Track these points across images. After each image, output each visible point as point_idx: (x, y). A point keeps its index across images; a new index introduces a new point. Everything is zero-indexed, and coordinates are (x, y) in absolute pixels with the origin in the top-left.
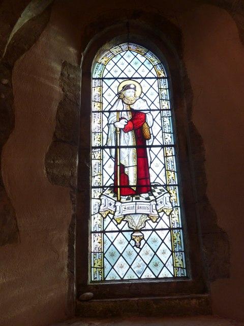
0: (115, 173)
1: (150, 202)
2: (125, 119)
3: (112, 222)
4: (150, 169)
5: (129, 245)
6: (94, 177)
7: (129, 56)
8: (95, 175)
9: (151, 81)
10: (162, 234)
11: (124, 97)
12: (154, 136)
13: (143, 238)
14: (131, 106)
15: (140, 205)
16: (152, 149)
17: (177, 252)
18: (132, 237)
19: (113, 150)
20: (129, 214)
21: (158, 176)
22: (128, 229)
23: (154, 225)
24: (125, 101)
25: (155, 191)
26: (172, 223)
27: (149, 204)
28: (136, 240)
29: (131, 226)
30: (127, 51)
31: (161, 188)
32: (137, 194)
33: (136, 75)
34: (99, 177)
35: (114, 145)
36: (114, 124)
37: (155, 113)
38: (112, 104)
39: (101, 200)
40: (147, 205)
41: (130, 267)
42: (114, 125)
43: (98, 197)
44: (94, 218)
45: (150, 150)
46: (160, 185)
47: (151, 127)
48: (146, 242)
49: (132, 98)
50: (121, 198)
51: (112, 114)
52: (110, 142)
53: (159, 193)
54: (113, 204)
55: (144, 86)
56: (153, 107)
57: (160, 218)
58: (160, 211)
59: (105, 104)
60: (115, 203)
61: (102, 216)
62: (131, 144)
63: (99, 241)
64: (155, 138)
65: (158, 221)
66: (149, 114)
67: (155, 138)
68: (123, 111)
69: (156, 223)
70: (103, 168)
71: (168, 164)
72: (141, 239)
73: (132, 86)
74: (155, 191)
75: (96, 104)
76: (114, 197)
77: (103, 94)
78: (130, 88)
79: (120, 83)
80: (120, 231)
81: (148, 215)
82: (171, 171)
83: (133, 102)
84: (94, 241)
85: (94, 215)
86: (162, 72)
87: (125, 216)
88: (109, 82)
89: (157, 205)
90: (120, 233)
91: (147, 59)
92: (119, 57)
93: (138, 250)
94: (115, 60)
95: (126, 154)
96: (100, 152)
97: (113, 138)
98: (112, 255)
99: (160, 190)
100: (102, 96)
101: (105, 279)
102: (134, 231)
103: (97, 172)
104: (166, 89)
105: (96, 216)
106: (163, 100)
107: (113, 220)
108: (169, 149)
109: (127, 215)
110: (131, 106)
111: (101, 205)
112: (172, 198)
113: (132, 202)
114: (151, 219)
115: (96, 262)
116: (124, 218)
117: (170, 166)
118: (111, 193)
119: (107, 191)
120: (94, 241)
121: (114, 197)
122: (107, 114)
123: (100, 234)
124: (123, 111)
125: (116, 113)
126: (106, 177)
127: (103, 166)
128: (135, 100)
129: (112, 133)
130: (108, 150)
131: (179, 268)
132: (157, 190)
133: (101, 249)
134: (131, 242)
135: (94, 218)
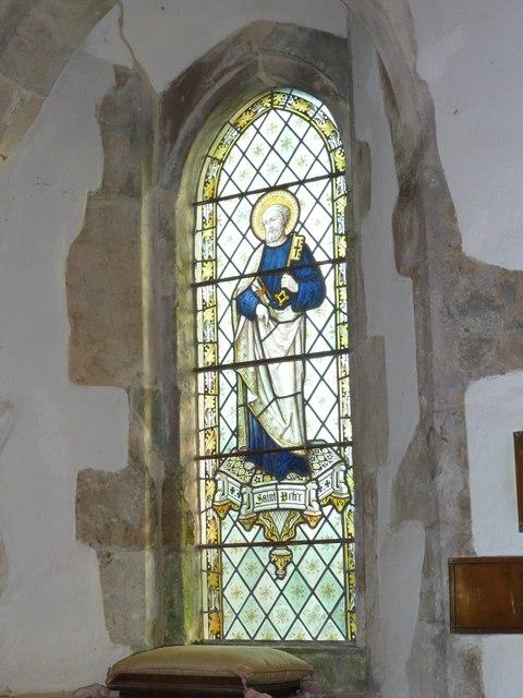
1: (304, 484)
10: (328, 551)
18: (270, 558)
20: (265, 511)
27: (303, 487)
28: (278, 564)
30: (268, 112)
33: (288, 178)
46: (327, 445)
48: (296, 569)
60: (241, 488)
72: (288, 563)
79: (254, 207)
81: (301, 511)
87: (258, 513)
89: (319, 489)
92: (251, 131)
102: (276, 545)
114: (306, 522)
134: (269, 569)
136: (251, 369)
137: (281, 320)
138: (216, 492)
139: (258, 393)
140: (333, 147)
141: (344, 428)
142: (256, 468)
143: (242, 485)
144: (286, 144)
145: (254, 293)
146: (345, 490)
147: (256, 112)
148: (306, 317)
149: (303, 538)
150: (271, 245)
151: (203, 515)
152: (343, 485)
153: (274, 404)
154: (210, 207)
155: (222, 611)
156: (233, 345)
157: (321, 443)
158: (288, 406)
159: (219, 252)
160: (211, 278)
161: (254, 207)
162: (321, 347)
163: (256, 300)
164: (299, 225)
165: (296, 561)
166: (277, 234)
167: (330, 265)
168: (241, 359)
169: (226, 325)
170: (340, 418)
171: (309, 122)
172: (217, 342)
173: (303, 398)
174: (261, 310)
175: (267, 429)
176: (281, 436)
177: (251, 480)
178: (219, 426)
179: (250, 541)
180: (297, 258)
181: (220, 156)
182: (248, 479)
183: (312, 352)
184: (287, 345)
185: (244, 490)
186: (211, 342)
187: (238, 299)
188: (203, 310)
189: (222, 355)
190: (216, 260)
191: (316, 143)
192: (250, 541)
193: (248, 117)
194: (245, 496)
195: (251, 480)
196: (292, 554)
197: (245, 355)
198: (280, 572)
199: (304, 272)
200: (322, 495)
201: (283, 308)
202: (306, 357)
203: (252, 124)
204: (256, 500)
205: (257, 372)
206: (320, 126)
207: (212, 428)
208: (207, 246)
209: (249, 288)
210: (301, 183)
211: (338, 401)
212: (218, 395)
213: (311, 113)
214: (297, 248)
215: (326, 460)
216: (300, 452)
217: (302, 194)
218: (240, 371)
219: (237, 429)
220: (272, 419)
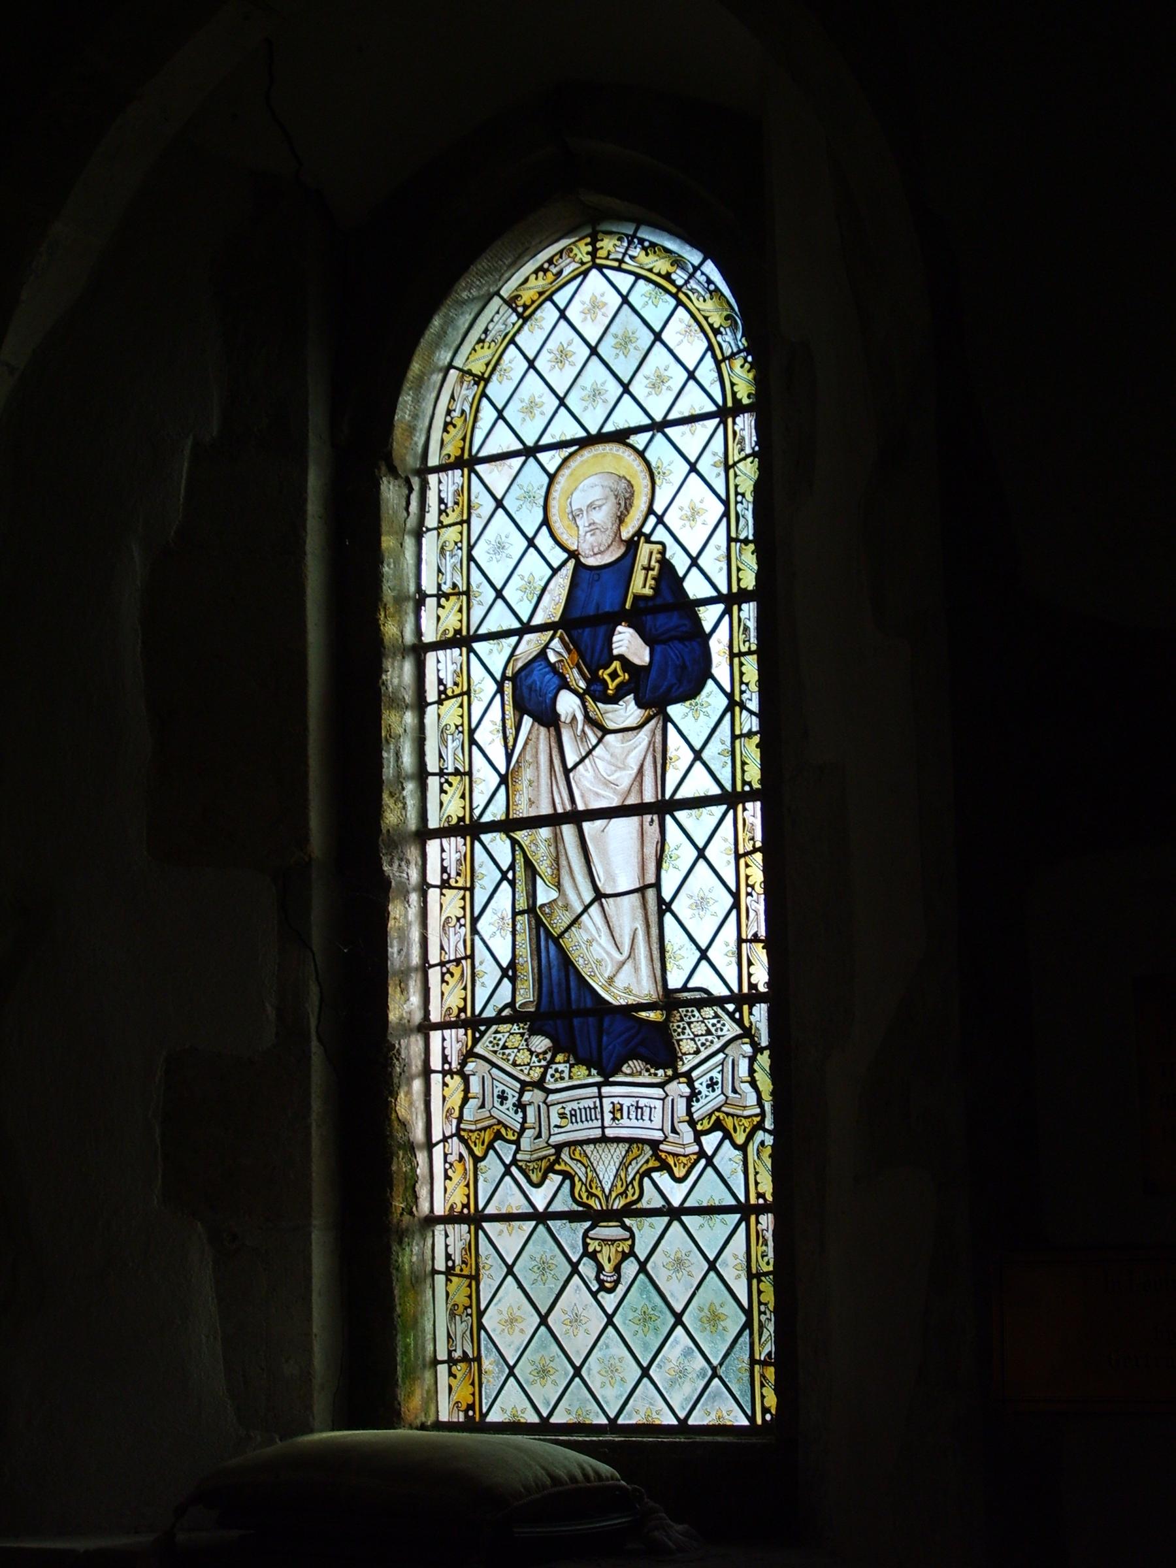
1: (661, 1085)
3: (508, 1179)
10: (711, 1232)
13: (632, 1253)
18: (585, 1245)
27: (658, 1092)
28: (603, 1258)
29: (584, 1195)
30: (585, 274)
33: (627, 416)
48: (643, 1268)
54: (511, 1101)
57: (703, 1162)
58: (706, 1125)
60: (521, 1093)
72: (625, 1256)
81: (654, 1144)
87: (559, 1148)
89: (694, 1095)
92: (548, 314)
102: (598, 1218)
107: (514, 1170)
114: (665, 1167)
116: (558, 1161)
126: (489, 974)
134: (581, 1268)
136: (545, 832)
137: (611, 725)
138: (465, 1100)
139: (559, 886)
140: (728, 352)
141: (750, 964)
142: (556, 1049)
143: (525, 1086)
144: (625, 343)
145: (553, 667)
146: (752, 1099)
147: (560, 273)
148: (667, 719)
149: (658, 1203)
150: (591, 562)
151: (438, 1152)
152: (746, 1088)
153: (594, 910)
154: (454, 479)
155: (478, 1359)
156: (504, 780)
157: (697, 995)
158: (626, 914)
159: (476, 575)
160: (458, 632)
161: (552, 478)
162: (699, 784)
163: (556, 681)
164: (652, 520)
165: (642, 1252)
166: (605, 538)
167: (719, 608)
168: (523, 810)
169: (489, 736)
170: (740, 941)
171: (675, 296)
172: (470, 774)
173: (660, 900)
174: (567, 704)
175: (580, 964)
176: (611, 980)
177: (544, 1075)
178: (472, 957)
179: (541, 1208)
180: (648, 591)
181: (478, 368)
182: (536, 1074)
183: (678, 796)
184: (625, 778)
185: (527, 1097)
186: (457, 772)
187: (514, 679)
188: (440, 702)
189: (480, 800)
190: (467, 593)
191: (692, 348)
192: (541, 1208)
193: (539, 283)
194: (531, 1112)
195: (544, 1075)
196: (632, 1236)
197: (531, 802)
198: (608, 1276)
199: (662, 622)
200: (700, 1109)
201: (614, 700)
202: (665, 807)
203: (550, 299)
204: (555, 1120)
205: (557, 839)
206: (700, 305)
207: (458, 961)
208: (449, 562)
209: (542, 654)
210: (658, 427)
211: (736, 905)
212: (471, 889)
213: (679, 277)
214: (648, 569)
215: (709, 1032)
216: (653, 1016)
217: (659, 451)
218: (520, 835)
219: (513, 964)
220: (590, 942)
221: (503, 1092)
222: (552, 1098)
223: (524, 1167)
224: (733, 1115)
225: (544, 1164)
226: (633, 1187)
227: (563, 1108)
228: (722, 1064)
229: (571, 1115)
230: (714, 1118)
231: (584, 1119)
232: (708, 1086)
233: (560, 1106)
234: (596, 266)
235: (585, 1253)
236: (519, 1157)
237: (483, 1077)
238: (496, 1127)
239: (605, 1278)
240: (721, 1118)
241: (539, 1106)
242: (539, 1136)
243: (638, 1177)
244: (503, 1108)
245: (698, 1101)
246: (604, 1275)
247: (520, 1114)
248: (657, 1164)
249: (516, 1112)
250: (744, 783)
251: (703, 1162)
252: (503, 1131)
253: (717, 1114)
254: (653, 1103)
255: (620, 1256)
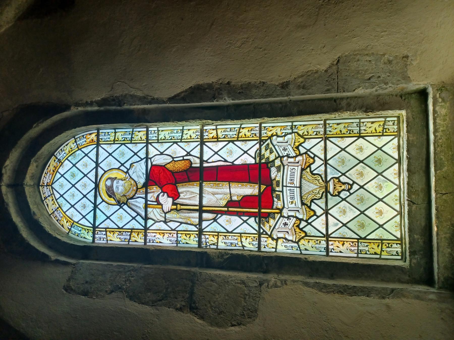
0: (239, 214)
1: (284, 166)
2: (158, 196)
3: (312, 224)
4: (235, 163)
5: (347, 199)
6: (243, 246)
7: (62, 186)
8: (241, 245)
9: (103, 154)
10: (332, 150)
11: (124, 196)
12: (186, 155)
14: (140, 186)
15: (288, 181)
16: (205, 158)
17: (360, 130)
18: (336, 195)
19: (205, 215)
20: (301, 197)
21: (245, 152)
22: (324, 200)
23: (318, 162)
24: (131, 196)
25: (268, 158)
26: (316, 134)
27: (286, 167)
28: (340, 189)
29: (318, 195)
30: (52, 188)
31: (263, 147)
32: (272, 185)
33: (92, 176)
34: (243, 239)
35: (197, 214)
36: (165, 213)
37: (152, 151)
38: (134, 214)
39: (279, 238)
40: (288, 171)
41: (380, 200)
42: (167, 212)
43: (274, 242)
44: (306, 250)
45: (206, 161)
46: (260, 149)
47: (173, 158)
49: (126, 184)
50: (277, 209)
51: (150, 215)
52: (193, 220)
53: (271, 152)
54: (286, 220)
55: (109, 164)
56: (142, 154)
57: (309, 153)
58: (297, 152)
59: (134, 224)
60: (284, 217)
61: (303, 238)
62: (196, 190)
63: (340, 245)
64: (188, 154)
65: (312, 156)
66: (152, 160)
67: (188, 154)
68: (146, 199)
69: (316, 158)
70: (231, 232)
71: (229, 136)
72: (339, 181)
73: (109, 183)
74: (268, 158)
75: (133, 239)
76: (274, 218)
77: (119, 228)
78: (112, 186)
79: (103, 201)
80: (327, 212)
81: (302, 170)
82: (239, 132)
83: (132, 182)
84: (341, 252)
85: (300, 250)
86: (88, 136)
87: (303, 204)
88: (100, 217)
89: (288, 156)
90: (330, 212)
91: (67, 159)
92: (61, 200)
93: (355, 187)
94: (66, 207)
95: (211, 197)
96: (207, 236)
97: (187, 215)
98: (362, 226)
99: (266, 150)
100: (122, 228)
101: (398, 239)
102: (327, 191)
103: (236, 242)
104: (115, 132)
105: (302, 247)
106: (132, 137)
107: (309, 221)
108: (207, 134)
109: (302, 201)
110: (140, 186)
111: (286, 239)
112: (279, 134)
113: (282, 192)
114: (309, 166)
115: (372, 251)
116: (307, 205)
117: (231, 133)
118: (268, 222)
119: (266, 228)
120: (341, 252)
121: (274, 218)
122: (150, 222)
123: (330, 243)
124: (146, 199)
125: (149, 210)
126: (245, 228)
127: (228, 232)
128: (131, 180)
129: (178, 216)
130: (205, 224)
131: (384, 128)
132: (267, 154)
133: (353, 242)
134: (344, 197)
135: (306, 250)
149: (323, 168)
152: (286, 138)
164: (122, 168)
167: (149, 145)
204: (293, 205)
221: (283, 224)
222: (286, 206)
223: (309, 217)
224: (295, 143)
225: (308, 210)
226: (316, 178)
227: (290, 202)
228: (279, 146)
229: (292, 199)
230: (295, 149)
231: (293, 194)
232: (285, 151)
233: (289, 203)
234: (51, 186)
235: (338, 195)
236: (305, 219)
237: (278, 232)
238: (295, 227)
239: (347, 188)
240: (295, 146)
241: (289, 210)
242: (298, 211)
243: (313, 176)
244: (289, 224)
245: (290, 154)
246: (346, 188)
247: (292, 218)
248: (309, 169)
249: (290, 219)
250: (198, 138)
251: (309, 153)
252: (296, 225)
253: (294, 148)
254: (289, 169)
255: (339, 183)
